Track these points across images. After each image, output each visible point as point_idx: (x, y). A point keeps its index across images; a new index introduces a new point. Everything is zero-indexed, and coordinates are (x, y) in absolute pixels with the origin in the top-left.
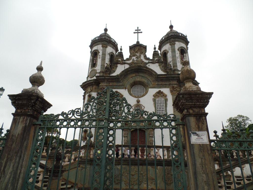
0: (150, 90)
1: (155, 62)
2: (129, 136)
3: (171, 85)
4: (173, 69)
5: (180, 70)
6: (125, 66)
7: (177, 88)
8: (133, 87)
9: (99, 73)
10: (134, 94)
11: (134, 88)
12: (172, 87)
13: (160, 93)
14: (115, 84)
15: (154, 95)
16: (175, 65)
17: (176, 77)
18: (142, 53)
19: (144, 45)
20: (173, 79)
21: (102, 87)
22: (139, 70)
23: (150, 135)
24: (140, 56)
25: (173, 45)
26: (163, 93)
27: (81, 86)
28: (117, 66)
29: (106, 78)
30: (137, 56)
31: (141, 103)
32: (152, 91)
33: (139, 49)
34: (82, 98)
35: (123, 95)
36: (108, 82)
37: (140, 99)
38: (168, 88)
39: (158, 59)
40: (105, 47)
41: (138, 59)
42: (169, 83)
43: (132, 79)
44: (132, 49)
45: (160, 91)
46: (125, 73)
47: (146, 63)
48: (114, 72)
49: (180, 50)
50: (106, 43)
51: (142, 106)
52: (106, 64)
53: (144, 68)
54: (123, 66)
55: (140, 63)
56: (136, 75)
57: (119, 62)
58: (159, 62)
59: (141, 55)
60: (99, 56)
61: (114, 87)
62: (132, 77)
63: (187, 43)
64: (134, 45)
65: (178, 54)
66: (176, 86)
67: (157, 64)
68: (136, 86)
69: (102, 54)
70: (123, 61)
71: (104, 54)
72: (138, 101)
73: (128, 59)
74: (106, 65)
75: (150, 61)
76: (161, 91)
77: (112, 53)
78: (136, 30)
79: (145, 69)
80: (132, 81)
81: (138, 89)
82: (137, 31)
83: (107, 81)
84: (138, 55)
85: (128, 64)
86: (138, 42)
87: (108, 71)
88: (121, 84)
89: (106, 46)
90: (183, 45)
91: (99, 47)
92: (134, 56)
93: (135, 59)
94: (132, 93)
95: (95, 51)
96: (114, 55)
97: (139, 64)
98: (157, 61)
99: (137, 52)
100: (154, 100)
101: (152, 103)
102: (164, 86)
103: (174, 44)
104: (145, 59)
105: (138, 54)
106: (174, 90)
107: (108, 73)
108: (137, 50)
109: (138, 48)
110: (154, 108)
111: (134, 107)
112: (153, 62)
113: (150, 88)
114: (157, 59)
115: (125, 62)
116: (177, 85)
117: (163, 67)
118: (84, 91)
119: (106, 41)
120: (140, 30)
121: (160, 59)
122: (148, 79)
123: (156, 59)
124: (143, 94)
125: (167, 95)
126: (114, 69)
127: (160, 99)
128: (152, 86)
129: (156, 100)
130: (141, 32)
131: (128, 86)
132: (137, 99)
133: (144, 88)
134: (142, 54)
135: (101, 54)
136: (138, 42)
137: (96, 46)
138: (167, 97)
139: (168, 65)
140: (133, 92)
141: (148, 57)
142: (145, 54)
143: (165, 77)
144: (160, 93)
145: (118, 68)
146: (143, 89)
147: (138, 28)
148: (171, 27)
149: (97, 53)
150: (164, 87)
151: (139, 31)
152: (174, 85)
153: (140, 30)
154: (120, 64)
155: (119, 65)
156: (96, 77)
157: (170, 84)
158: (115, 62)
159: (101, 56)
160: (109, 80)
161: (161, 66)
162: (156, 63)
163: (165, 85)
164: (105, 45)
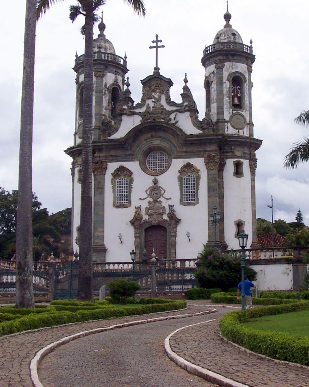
0: (174, 161)
1: (183, 110)
2: (143, 235)
3: (207, 153)
6: (134, 119)
10: (152, 168)
11: (152, 156)
13: (189, 166)
14: (120, 153)
15: (179, 171)
16: (220, 111)
17: (214, 139)
18: (162, 92)
19: (165, 77)
23: (172, 234)
24: (159, 100)
25: (220, 68)
27: (65, 151)
29: (104, 144)
30: (155, 98)
31: (160, 184)
32: (178, 164)
33: (157, 84)
34: (70, 172)
35: (132, 173)
36: (107, 149)
37: (159, 178)
38: (202, 157)
39: (188, 104)
42: (204, 149)
43: (144, 144)
44: (146, 86)
45: (190, 163)
47: (169, 111)
48: (117, 130)
50: (102, 67)
51: (161, 189)
54: (131, 118)
56: (152, 136)
57: (125, 112)
59: (160, 97)
61: (118, 158)
62: (145, 140)
63: (249, 58)
64: (149, 78)
65: (227, 85)
66: (213, 154)
67: (188, 114)
68: (154, 153)
70: (131, 109)
72: (155, 182)
73: (139, 106)
75: (174, 108)
78: (153, 42)
79: (165, 125)
80: (146, 146)
82: (155, 44)
83: (107, 148)
84: (156, 97)
85: (141, 116)
86: (157, 69)
88: (129, 152)
89: (103, 74)
90: (241, 67)
92: (149, 98)
93: (152, 105)
94: (147, 166)
96: (119, 86)
97: (157, 114)
98: (187, 108)
99: (153, 90)
100: (180, 179)
102: (197, 153)
103: (221, 68)
104: (168, 105)
106: (211, 161)
107: (107, 132)
108: (154, 86)
109: (156, 83)
110: (180, 191)
111: (149, 190)
112: (181, 109)
113: (174, 158)
120: (161, 41)
121: (192, 106)
122: (172, 143)
123: (186, 104)
125: (199, 170)
126: (117, 124)
127: (189, 176)
128: (178, 154)
129: (183, 178)
130: (163, 46)
131: (140, 156)
132: (153, 178)
133: (167, 157)
134: (163, 94)
136: (157, 69)
138: (200, 173)
140: (149, 163)
141: (172, 99)
143: (198, 140)
144: (189, 166)
145: (123, 123)
146: (166, 157)
147: (157, 36)
148: (228, 17)
150: (196, 156)
151: (159, 44)
152: (211, 153)
153: (161, 41)
154: (125, 114)
155: (124, 118)
157: (206, 151)
160: (109, 147)
161: (192, 118)
162: (187, 111)
163: (199, 151)
164: (100, 74)
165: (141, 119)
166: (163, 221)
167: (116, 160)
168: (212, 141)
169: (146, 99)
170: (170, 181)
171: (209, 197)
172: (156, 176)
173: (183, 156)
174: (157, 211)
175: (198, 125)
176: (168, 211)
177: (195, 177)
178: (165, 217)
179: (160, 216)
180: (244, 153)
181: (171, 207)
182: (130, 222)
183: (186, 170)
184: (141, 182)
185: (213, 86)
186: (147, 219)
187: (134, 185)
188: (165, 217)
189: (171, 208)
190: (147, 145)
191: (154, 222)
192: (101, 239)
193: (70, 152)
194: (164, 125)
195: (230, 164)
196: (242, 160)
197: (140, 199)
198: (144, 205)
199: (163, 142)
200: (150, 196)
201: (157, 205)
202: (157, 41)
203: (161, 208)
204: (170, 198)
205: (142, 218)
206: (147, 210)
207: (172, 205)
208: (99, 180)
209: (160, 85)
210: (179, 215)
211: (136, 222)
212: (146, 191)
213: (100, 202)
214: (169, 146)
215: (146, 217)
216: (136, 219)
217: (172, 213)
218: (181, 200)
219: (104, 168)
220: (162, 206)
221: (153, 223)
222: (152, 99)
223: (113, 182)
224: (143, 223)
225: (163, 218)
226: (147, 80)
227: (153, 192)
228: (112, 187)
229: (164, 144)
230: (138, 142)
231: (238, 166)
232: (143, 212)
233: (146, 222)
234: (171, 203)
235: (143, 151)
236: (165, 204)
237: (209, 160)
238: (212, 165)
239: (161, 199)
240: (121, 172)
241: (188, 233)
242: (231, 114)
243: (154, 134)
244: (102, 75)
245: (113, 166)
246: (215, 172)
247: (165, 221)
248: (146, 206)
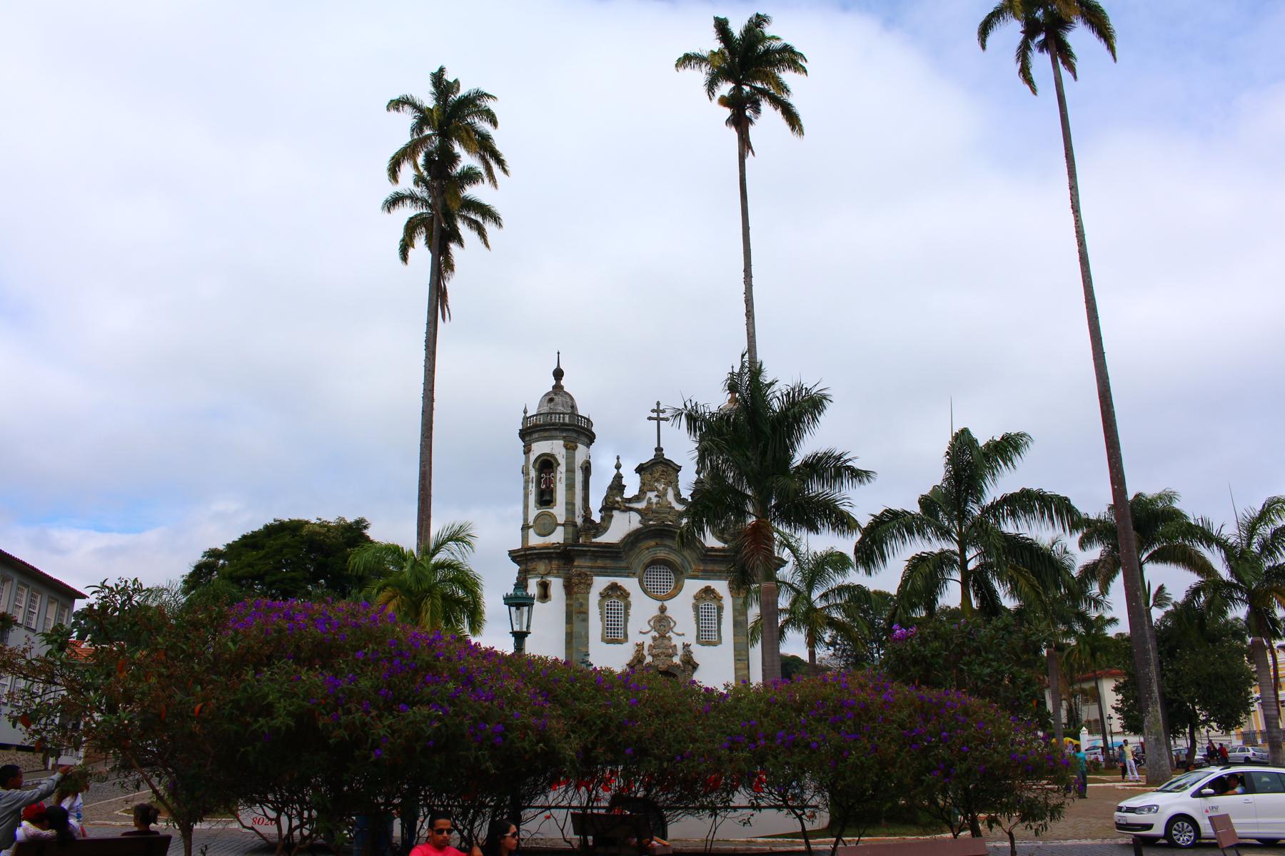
13: (708, 591)
14: (609, 563)
18: (669, 484)
24: (665, 494)
31: (668, 613)
32: (692, 586)
40: (571, 448)
50: (574, 435)
54: (626, 515)
60: (558, 476)
69: (567, 471)
71: (570, 470)
72: (663, 609)
73: (637, 499)
78: (653, 411)
81: (661, 578)
82: (655, 415)
84: (661, 487)
86: (659, 449)
88: (623, 564)
91: (555, 447)
93: (654, 500)
100: (696, 608)
101: (692, 614)
118: (517, 568)
119: (574, 430)
120: (663, 411)
131: (639, 571)
132: (659, 603)
135: (562, 469)
136: (659, 449)
142: (677, 486)
144: (708, 591)
145: (614, 520)
147: (658, 404)
151: (662, 415)
153: (663, 411)
155: (615, 513)
159: (564, 476)
165: (638, 517)
170: (681, 608)
176: (680, 652)
178: (676, 660)
181: (686, 646)
184: (642, 608)
187: (631, 611)
188: (676, 660)
191: (662, 667)
193: (515, 556)
198: (648, 641)
200: (654, 628)
201: (666, 642)
202: (657, 411)
215: (649, 659)
223: (601, 606)
229: (673, 557)
230: (637, 550)
232: (646, 652)
233: (649, 665)
236: (677, 642)
239: (671, 634)
240: (614, 591)
243: (658, 541)
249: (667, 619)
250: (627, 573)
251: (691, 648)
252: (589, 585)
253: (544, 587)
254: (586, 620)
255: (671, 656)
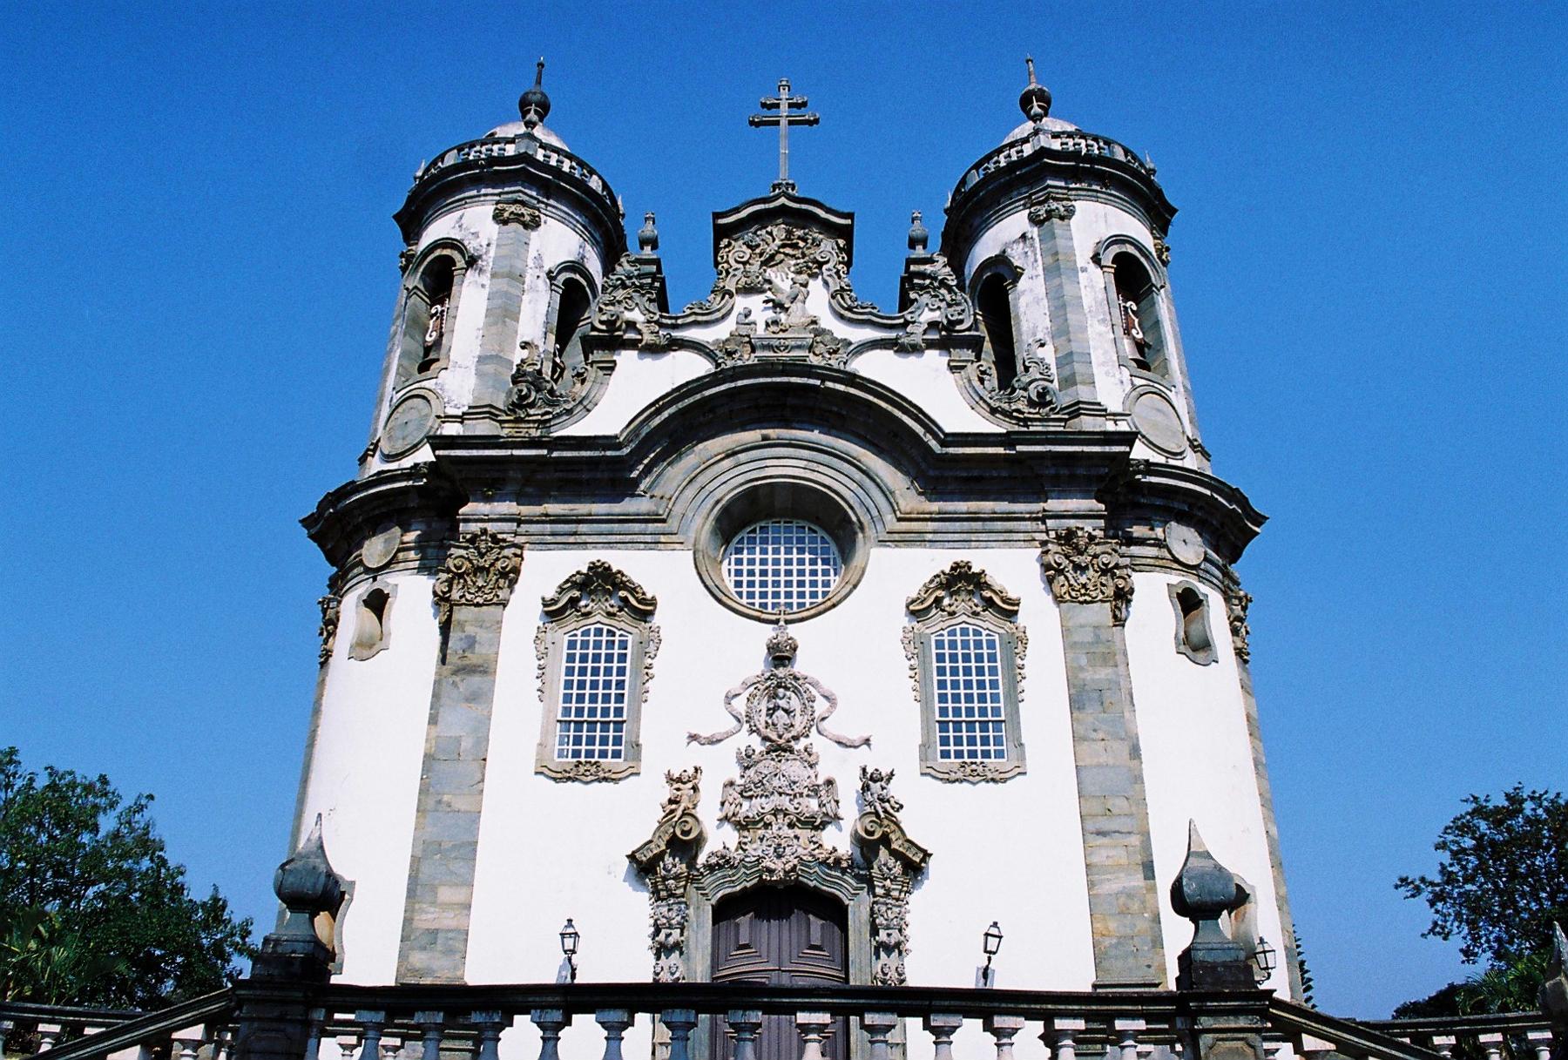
3: (1049, 522)
4: (1064, 399)
5: (1114, 406)
7: (1099, 549)
8: (736, 534)
9: (461, 419)
12: (1058, 537)
13: (962, 580)
20: (1064, 471)
21: (475, 527)
22: (791, 401)
23: (883, 936)
26: (989, 587)
27: (306, 522)
28: (610, 368)
29: (516, 452)
33: (789, 233)
35: (653, 602)
41: (783, 317)
46: (680, 424)
49: (1107, 259)
52: (525, 345)
53: (830, 384)
55: (799, 347)
56: (765, 438)
58: (946, 338)
59: (805, 285)
61: (583, 528)
65: (1095, 285)
67: (935, 359)
72: (781, 655)
74: (519, 355)
76: (976, 569)
77: (576, 266)
79: (841, 387)
87: (532, 405)
92: (749, 290)
95: (438, 252)
99: (772, 257)
100: (915, 645)
102: (999, 525)
104: (842, 317)
105: (782, 279)
108: (778, 242)
111: (746, 694)
114: (936, 316)
115: (677, 334)
116: (1102, 523)
117: (982, 381)
123: (927, 316)
124: (825, 594)
126: (588, 385)
129: (933, 638)
131: (701, 525)
132: (768, 631)
133: (833, 548)
134: (813, 276)
137: (450, 211)
139: (1027, 369)
144: (962, 580)
149: (450, 261)
152: (1072, 523)
154: (632, 344)
155: (626, 359)
156: (438, 442)
158: (594, 328)
162: (931, 345)
166: (824, 863)
167: (572, 539)
168: (1081, 471)
169: (738, 290)
171: (1077, 739)
172: (787, 622)
173: (930, 537)
174: (784, 802)
175: (995, 404)
177: (997, 637)
179: (805, 834)
180: (1206, 559)
181: (871, 779)
182: (632, 857)
183: (946, 601)
185: (1023, 284)
186: (733, 845)
187: (659, 665)
188: (839, 841)
189: (876, 787)
190: (741, 479)
192: (449, 952)
194: (830, 384)
195: (1152, 593)
196: (1202, 588)
197: (693, 737)
198: (719, 768)
199: (821, 469)
201: (793, 768)
203: (815, 791)
204: (867, 742)
205: (699, 841)
206: (734, 794)
207: (885, 772)
208: (470, 630)
209: (801, 244)
210: (916, 825)
211: (666, 862)
212: (729, 698)
213: (466, 744)
214: (854, 486)
216: (669, 844)
217: (886, 811)
218: (925, 747)
219: (503, 574)
220: (820, 781)
221: (771, 871)
222: (764, 291)
224: (711, 868)
225: (828, 846)
226: (744, 214)
227: (764, 706)
228: (540, 668)
231: (1189, 602)
232: (708, 812)
233: (722, 863)
234: (875, 760)
235: (717, 502)
237: (1067, 557)
238: (1083, 580)
241: (994, 931)
242: (1128, 387)
244: (527, 218)
245: (546, 570)
246: (1102, 613)
247: (838, 861)
248: (725, 780)
249: (795, 685)
250: (654, 529)
251: (895, 790)
252: (510, 576)
253: (377, 603)
254: (481, 697)
255: (813, 824)
